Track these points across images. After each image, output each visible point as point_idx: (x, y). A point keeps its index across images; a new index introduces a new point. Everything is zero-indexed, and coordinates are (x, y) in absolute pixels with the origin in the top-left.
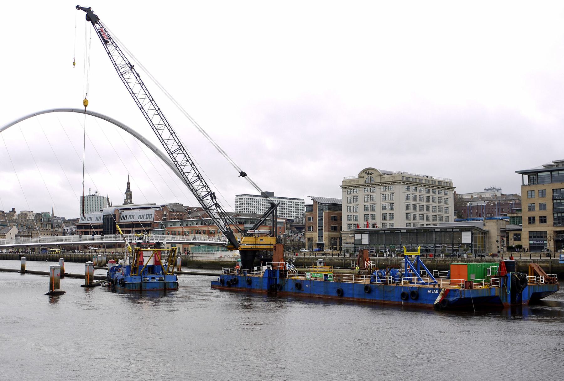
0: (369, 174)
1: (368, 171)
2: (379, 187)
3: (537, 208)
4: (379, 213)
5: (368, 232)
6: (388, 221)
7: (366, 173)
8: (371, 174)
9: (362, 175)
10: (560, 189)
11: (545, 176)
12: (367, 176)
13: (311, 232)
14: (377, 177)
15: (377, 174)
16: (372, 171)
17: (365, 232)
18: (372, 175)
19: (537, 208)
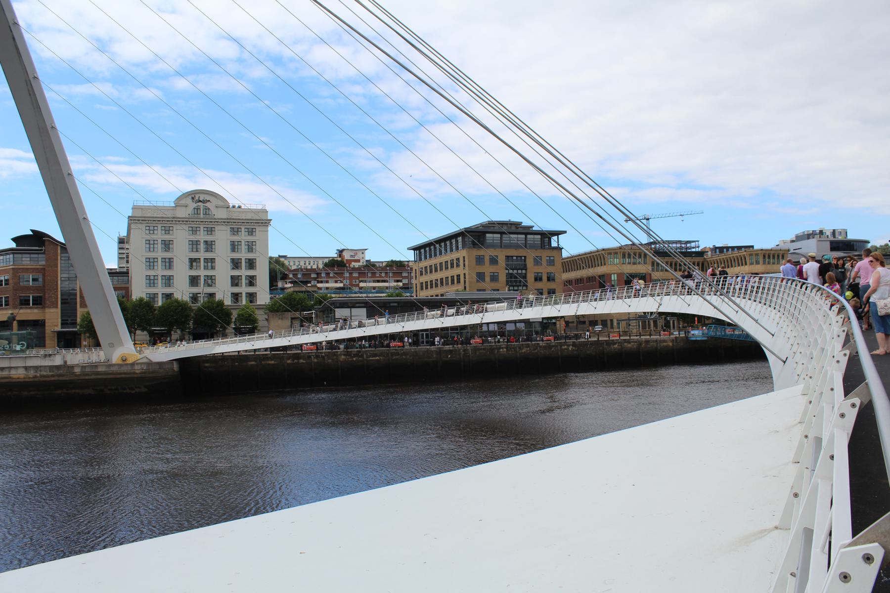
0: (200, 201)
1: (199, 195)
2: (224, 228)
3: (488, 279)
4: (223, 273)
5: (363, 305)
6: (244, 289)
7: (193, 198)
8: (204, 202)
9: (183, 202)
10: (512, 257)
11: (494, 239)
12: (195, 205)
13: (31, 308)
14: (219, 209)
15: (220, 203)
16: (207, 198)
17: (357, 305)
18: (208, 205)
19: (488, 279)
